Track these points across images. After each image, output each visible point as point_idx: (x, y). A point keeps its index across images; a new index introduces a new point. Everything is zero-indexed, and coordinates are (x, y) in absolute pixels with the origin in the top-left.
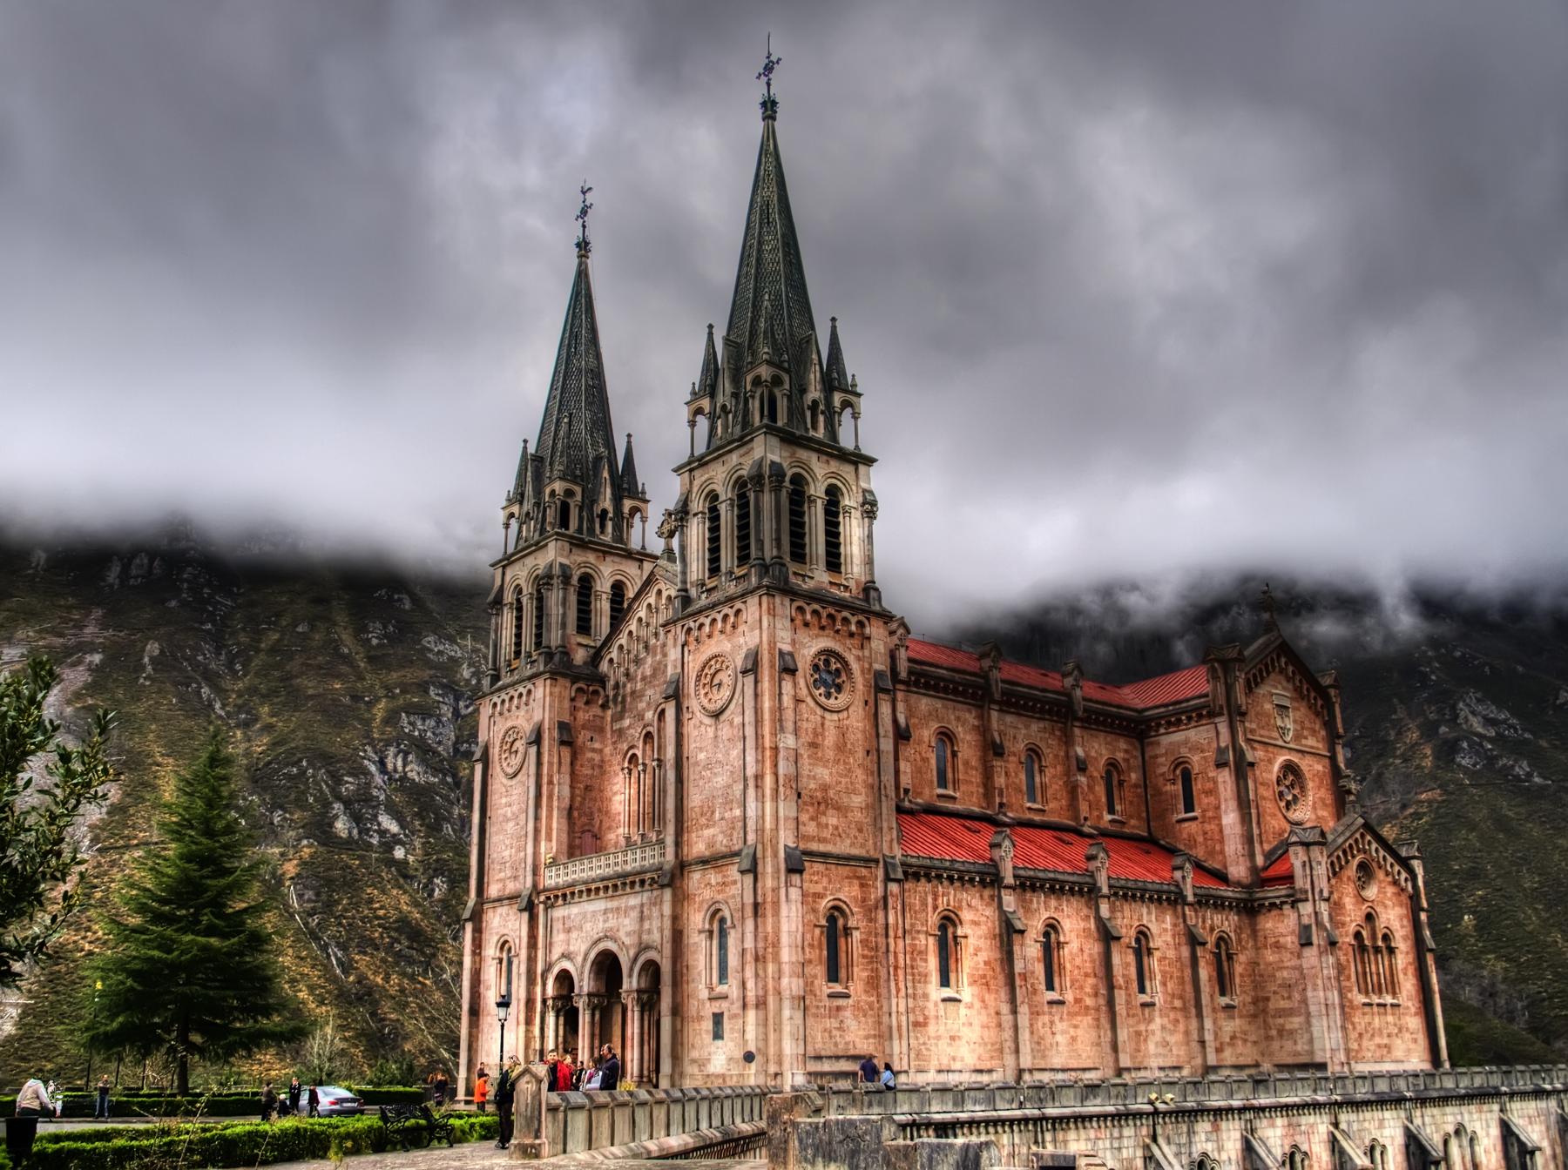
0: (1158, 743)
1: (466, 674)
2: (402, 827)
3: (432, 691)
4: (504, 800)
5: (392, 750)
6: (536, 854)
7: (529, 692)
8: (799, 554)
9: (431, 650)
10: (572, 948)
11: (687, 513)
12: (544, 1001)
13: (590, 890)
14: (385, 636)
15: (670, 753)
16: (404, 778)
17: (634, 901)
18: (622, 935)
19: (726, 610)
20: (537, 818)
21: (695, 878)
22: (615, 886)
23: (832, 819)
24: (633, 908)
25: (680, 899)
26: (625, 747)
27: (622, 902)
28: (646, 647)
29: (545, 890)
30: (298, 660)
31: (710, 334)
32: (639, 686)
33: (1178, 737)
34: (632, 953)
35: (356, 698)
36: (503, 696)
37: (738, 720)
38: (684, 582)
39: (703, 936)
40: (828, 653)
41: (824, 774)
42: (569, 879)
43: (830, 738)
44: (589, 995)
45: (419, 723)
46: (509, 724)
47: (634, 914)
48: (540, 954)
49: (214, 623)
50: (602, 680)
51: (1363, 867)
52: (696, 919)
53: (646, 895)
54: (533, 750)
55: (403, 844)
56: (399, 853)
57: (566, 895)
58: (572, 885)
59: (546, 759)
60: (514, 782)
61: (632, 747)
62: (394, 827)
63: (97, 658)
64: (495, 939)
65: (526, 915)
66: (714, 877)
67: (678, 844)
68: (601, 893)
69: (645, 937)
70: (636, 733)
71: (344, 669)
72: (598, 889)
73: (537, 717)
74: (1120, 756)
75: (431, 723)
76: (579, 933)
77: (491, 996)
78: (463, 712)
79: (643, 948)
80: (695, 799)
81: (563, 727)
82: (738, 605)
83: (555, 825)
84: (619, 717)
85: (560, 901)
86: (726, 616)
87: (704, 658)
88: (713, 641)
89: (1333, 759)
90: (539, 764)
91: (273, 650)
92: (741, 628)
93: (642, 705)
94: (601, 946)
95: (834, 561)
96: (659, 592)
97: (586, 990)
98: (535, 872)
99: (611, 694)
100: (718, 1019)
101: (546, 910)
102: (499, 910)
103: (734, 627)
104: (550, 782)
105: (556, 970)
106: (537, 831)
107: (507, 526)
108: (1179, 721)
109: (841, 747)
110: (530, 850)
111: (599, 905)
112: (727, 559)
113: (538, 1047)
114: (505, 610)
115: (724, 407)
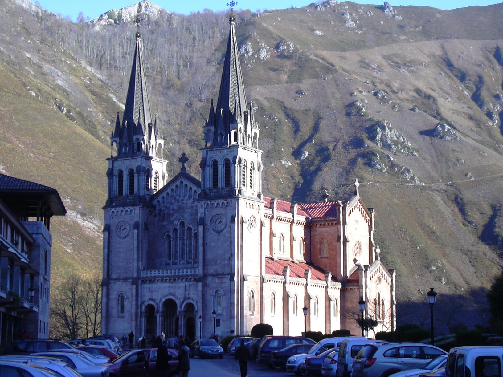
0: (316, 231)
4: (118, 246)
6: (138, 266)
7: (131, 210)
10: (153, 297)
11: (205, 165)
12: (141, 313)
13: (163, 280)
15: (201, 241)
17: (183, 284)
18: (177, 294)
19: (223, 201)
20: (138, 254)
21: (209, 280)
22: (175, 280)
24: (181, 287)
25: (205, 285)
26: (164, 231)
27: (177, 285)
28: (175, 199)
29: (141, 278)
31: (212, 103)
32: (171, 212)
33: (324, 229)
34: (182, 300)
36: (117, 209)
37: (228, 235)
38: (204, 187)
39: (212, 297)
42: (153, 275)
44: (162, 312)
46: (121, 220)
47: (183, 288)
48: (140, 299)
50: (154, 207)
51: (379, 277)
52: (210, 292)
53: (187, 283)
54: (136, 231)
57: (152, 280)
58: (156, 277)
59: (140, 234)
60: (124, 240)
61: (168, 232)
64: (116, 293)
65: (134, 286)
66: (217, 281)
67: (204, 269)
68: (168, 281)
69: (187, 296)
70: (171, 228)
72: (166, 280)
73: (136, 219)
76: (158, 293)
77: (114, 311)
79: (185, 299)
80: (209, 256)
81: (146, 224)
82: (228, 200)
83: (144, 257)
84: (163, 220)
85: (148, 282)
86: (223, 203)
87: (214, 214)
88: (217, 209)
89: (370, 238)
90: (138, 236)
92: (228, 208)
93: (172, 219)
94: (167, 298)
96: (182, 182)
97: (160, 310)
98: (138, 272)
99: (158, 212)
100: (218, 321)
101: (141, 284)
102: (118, 283)
103: (226, 206)
104: (142, 243)
105: (146, 304)
106: (138, 258)
107: (112, 145)
108: (324, 224)
110: (135, 264)
111: (167, 285)
112: (221, 183)
113: (139, 327)
114: (114, 178)
115: (221, 134)
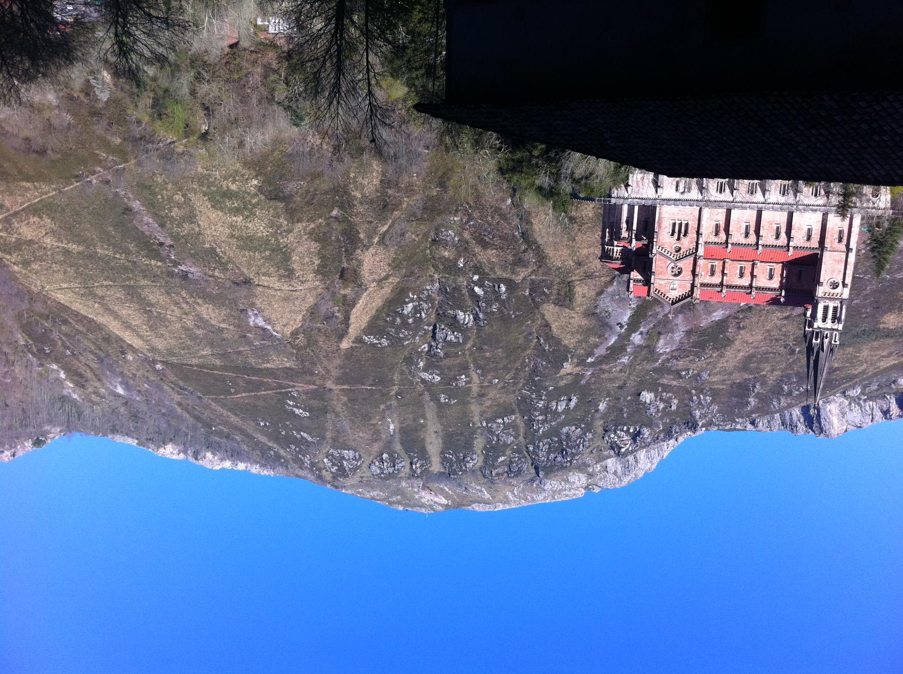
1: (422, 364)
2: (473, 289)
3: (442, 354)
5: (470, 325)
8: (835, 308)
9: (437, 375)
14: (457, 380)
16: (465, 312)
23: (837, 258)
30: (501, 366)
35: (480, 349)
40: (833, 288)
41: (838, 266)
43: (836, 273)
45: (453, 338)
49: (534, 381)
55: (473, 282)
56: (476, 278)
62: (476, 289)
63: (590, 360)
71: (482, 363)
74: (708, 277)
75: (448, 338)
78: (426, 345)
91: (509, 370)
95: (826, 308)
109: (833, 271)
